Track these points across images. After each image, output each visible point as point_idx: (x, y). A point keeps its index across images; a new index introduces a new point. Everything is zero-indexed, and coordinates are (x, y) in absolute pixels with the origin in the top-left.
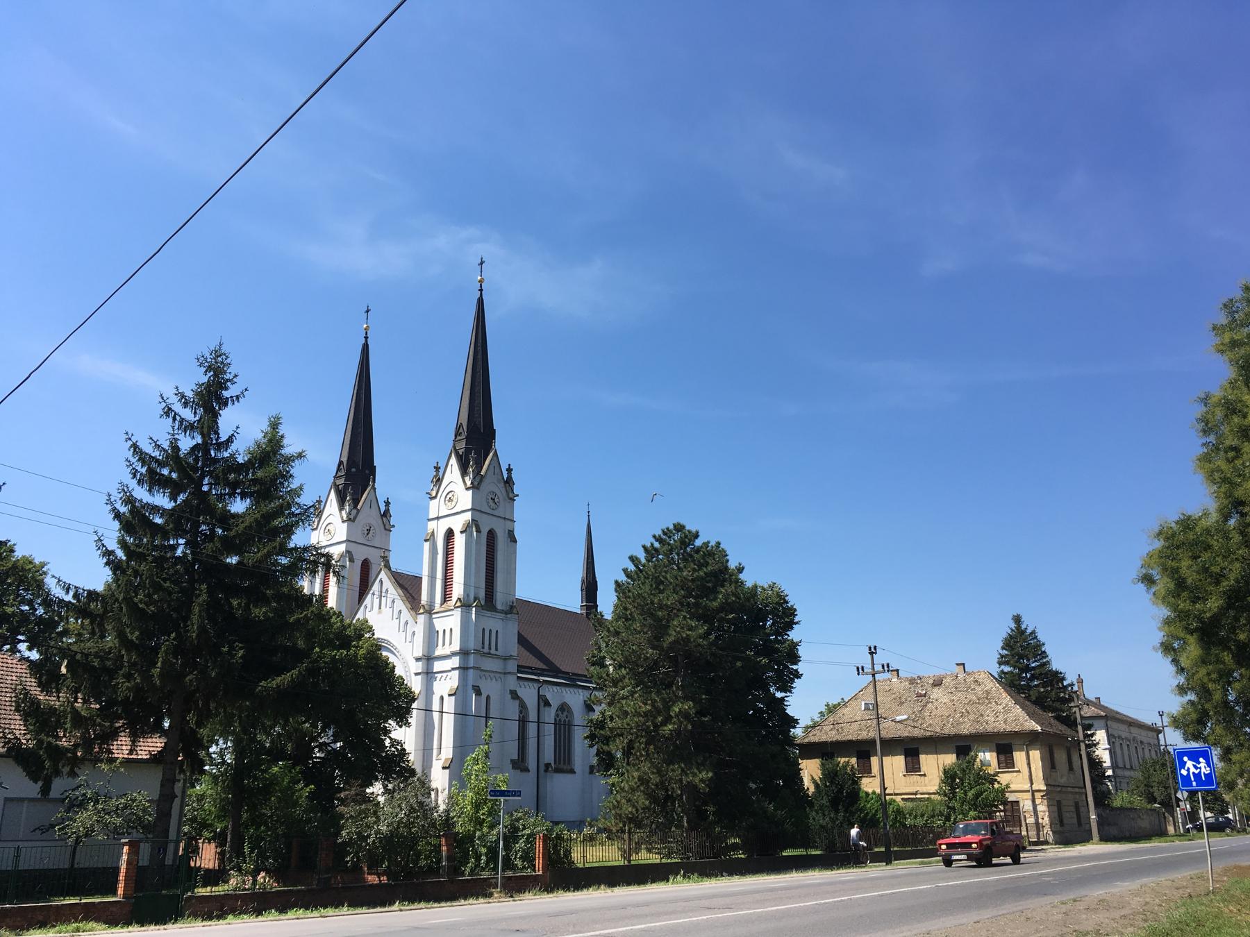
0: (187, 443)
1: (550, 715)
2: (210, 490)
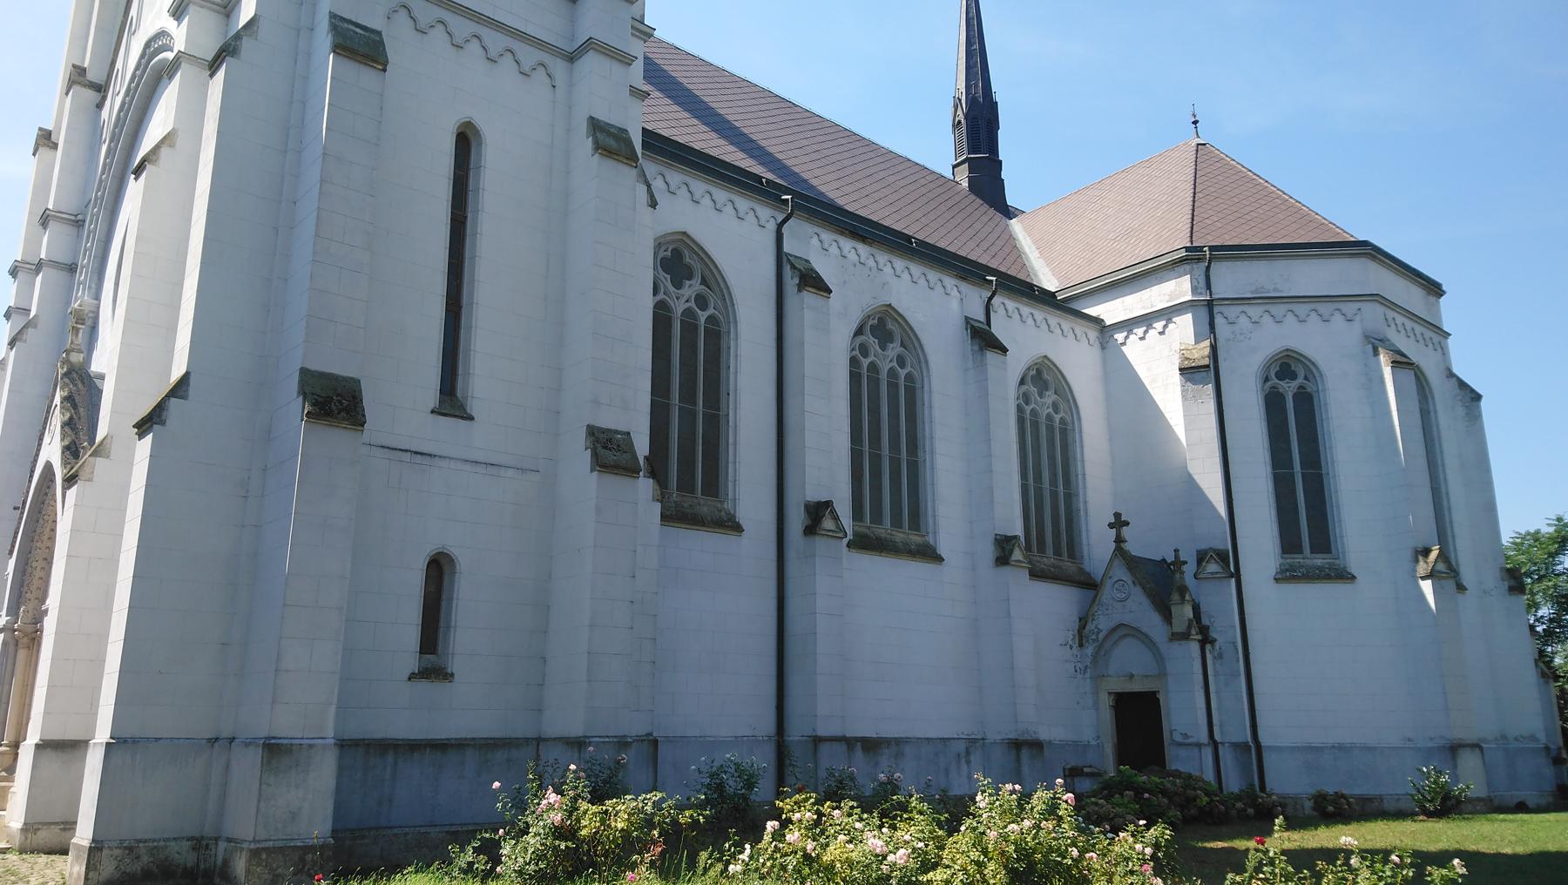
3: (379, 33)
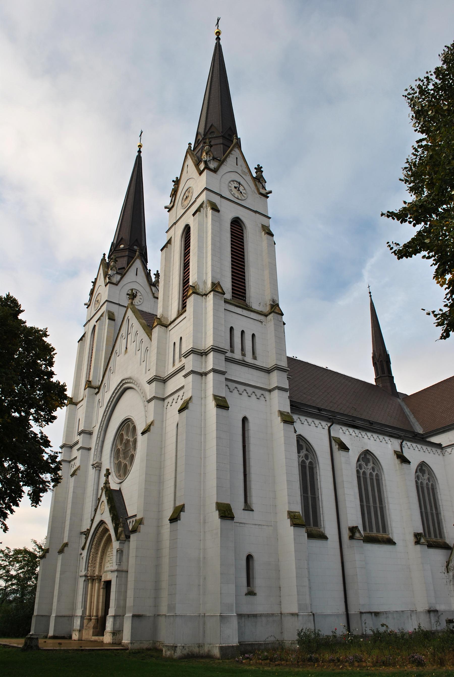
1: (348, 464)
3: (224, 398)
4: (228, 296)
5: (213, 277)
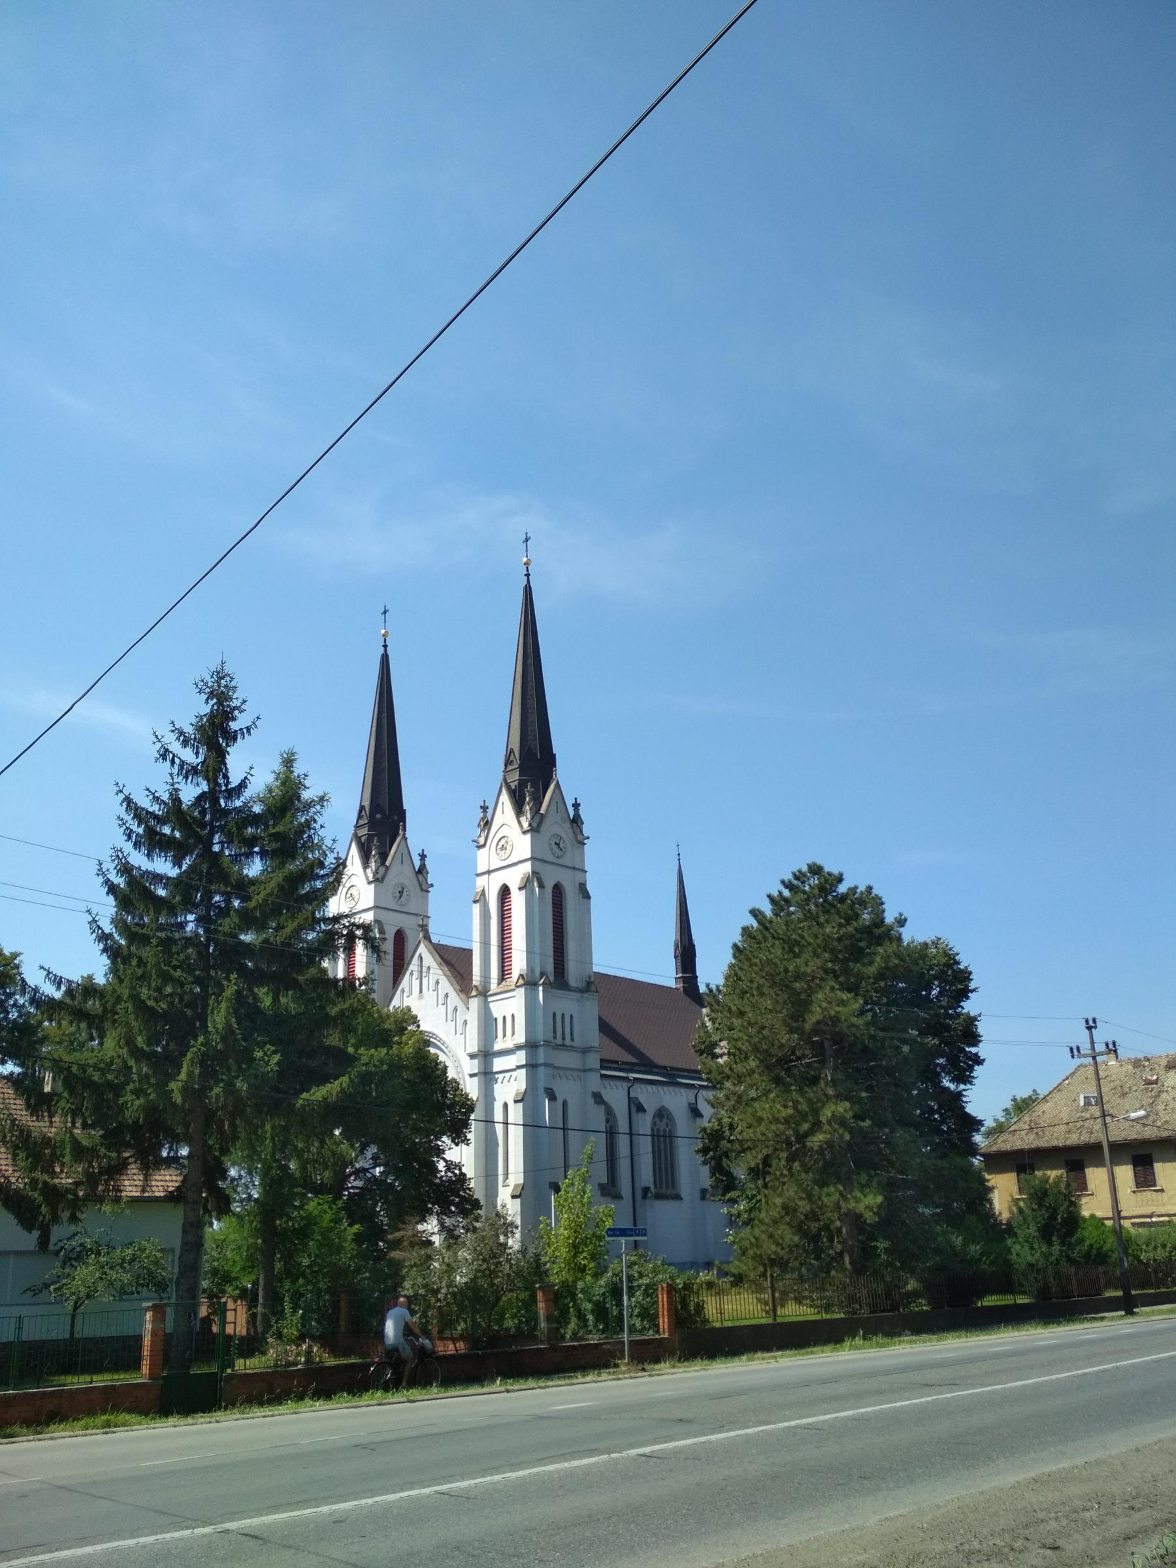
0: (189, 792)
1: (645, 1124)
2: (222, 850)
4: (552, 979)
5: (541, 967)
